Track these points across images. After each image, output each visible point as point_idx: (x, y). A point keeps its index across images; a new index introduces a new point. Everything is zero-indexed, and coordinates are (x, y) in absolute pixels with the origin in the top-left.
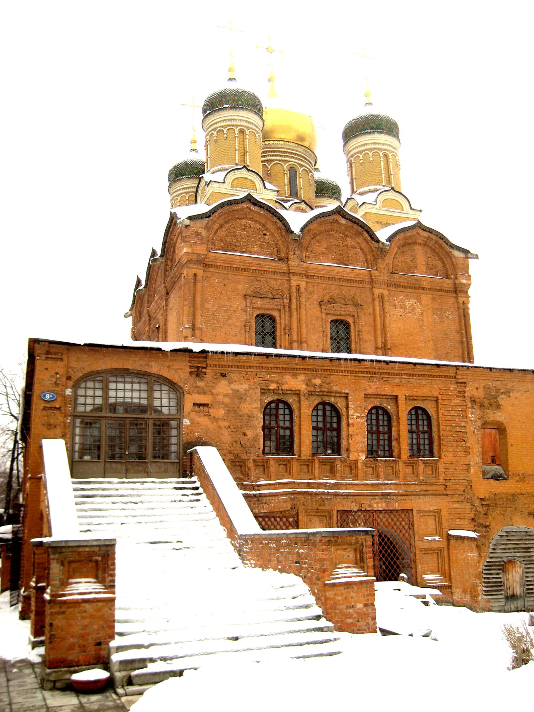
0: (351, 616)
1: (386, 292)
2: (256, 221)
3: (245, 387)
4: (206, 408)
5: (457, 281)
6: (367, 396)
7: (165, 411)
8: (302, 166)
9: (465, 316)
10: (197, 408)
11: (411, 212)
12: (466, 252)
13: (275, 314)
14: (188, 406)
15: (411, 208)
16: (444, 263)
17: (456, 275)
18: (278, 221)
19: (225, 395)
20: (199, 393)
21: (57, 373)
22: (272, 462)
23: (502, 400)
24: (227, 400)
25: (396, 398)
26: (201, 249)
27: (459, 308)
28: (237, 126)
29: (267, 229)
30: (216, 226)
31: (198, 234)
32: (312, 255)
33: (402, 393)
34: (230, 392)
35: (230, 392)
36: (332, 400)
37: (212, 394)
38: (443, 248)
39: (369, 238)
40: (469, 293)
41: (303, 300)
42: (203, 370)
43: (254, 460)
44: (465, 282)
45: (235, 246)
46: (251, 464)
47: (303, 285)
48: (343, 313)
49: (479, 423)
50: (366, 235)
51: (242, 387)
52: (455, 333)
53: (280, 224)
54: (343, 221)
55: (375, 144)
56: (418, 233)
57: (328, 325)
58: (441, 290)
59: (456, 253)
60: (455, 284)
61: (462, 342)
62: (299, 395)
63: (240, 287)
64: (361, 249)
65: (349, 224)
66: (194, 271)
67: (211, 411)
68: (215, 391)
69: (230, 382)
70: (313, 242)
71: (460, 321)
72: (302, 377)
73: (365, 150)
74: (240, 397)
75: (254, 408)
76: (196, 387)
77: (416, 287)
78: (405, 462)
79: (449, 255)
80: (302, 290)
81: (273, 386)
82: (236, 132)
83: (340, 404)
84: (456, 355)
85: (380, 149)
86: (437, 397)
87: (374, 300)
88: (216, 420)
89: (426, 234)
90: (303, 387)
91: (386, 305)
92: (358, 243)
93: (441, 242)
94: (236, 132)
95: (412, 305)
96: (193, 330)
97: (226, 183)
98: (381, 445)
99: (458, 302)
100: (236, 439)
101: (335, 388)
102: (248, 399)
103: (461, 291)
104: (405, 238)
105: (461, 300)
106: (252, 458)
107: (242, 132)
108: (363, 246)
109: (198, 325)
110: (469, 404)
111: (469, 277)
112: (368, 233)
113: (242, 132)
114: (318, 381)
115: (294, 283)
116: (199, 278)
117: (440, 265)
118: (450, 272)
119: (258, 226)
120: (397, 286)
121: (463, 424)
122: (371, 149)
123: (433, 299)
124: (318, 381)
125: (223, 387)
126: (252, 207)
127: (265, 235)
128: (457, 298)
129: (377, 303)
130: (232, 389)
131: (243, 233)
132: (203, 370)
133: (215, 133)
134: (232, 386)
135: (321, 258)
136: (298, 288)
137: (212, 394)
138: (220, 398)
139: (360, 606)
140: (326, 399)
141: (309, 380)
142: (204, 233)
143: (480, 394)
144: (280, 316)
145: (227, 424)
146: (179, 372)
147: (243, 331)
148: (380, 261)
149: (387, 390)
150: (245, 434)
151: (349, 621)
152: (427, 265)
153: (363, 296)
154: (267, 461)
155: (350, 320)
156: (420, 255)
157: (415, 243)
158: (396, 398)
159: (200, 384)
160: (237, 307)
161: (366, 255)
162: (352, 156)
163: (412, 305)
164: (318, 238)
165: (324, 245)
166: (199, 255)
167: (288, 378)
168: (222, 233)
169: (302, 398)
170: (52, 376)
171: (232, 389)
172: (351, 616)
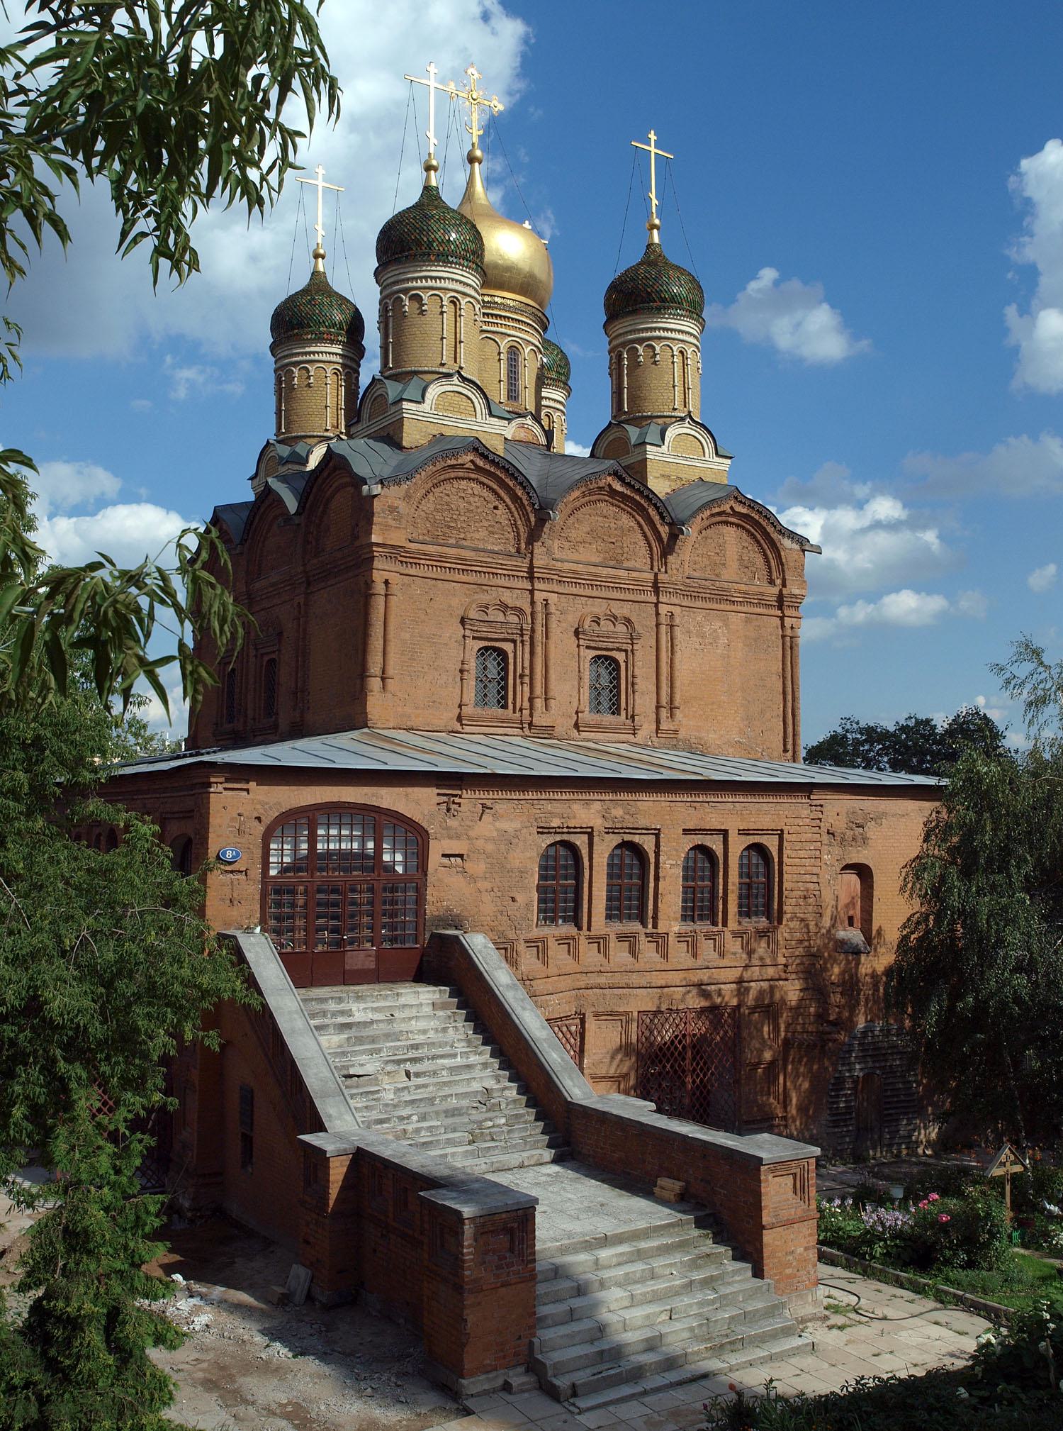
0: (789, 1265)
1: (676, 610)
2: (482, 483)
3: (517, 825)
4: (459, 860)
5: (785, 592)
6: (686, 831)
7: (399, 869)
10: (446, 861)
13: (508, 647)
14: (434, 859)
15: (717, 454)
19: (487, 840)
20: (450, 838)
21: (240, 815)
22: (552, 943)
23: (871, 830)
24: (490, 847)
25: (725, 833)
27: (783, 637)
30: (419, 495)
31: (393, 509)
32: (567, 545)
33: (733, 825)
34: (495, 834)
35: (495, 834)
36: (636, 839)
37: (469, 838)
41: (553, 624)
42: (457, 800)
43: (526, 941)
45: (449, 527)
46: (521, 947)
47: (553, 598)
48: (610, 646)
49: (839, 866)
51: (510, 826)
52: (775, 678)
57: (587, 665)
59: (787, 543)
62: (591, 835)
63: (455, 602)
66: (386, 575)
67: (467, 865)
68: (471, 833)
69: (496, 817)
70: (572, 519)
72: (597, 806)
74: (509, 841)
75: (528, 856)
76: (448, 828)
77: (723, 596)
78: (733, 932)
80: (552, 609)
81: (555, 823)
83: (648, 843)
84: (775, 714)
86: (782, 830)
87: (658, 625)
88: (473, 879)
90: (598, 823)
91: (677, 631)
95: (715, 631)
96: (383, 679)
97: (428, 401)
98: (702, 906)
100: (501, 908)
101: (643, 822)
102: (521, 844)
106: (522, 937)
107: (454, 302)
109: (391, 671)
110: (825, 838)
112: (657, 508)
114: (618, 812)
115: (539, 596)
116: (394, 588)
118: (774, 576)
119: (485, 493)
121: (815, 870)
123: (747, 621)
124: (618, 812)
125: (487, 827)
126: (480, 463)
127: (496, 508)
128: (782, 619)
129: (663, 629)
130: (497, 830)
131: (462, 504)
132: (457, 800)
134: (497, 824)
135: (581, 550)
136: (546, 604)
137: (469, 838)
138: (480, 843)
139: (800, 1250)
140: (627, 838)
141: (607, 810)
142: (403, 507)
143: (840, 825)
144: (515, 653)
145: (487, 885)
146: (417, 803)
147: (458, 679)
149: (714, 822)
150: (513, 900)
151: (789, 1271)
152: (741, 559)
153: (643, 619)
154: (543, 941)
155: (620, 657)
158: (725, 833)
159: (452, 823)
160: (450, 638)
162: (623, 345)
163: (715, 631)
164: (579, 515)
165: (586, 527)
166: (392, 547)
167: (576, 807)
168: (428, 505)
169: (596, 839)
170: (232, 819)
171: (497, 830)
172: (789, 1265)
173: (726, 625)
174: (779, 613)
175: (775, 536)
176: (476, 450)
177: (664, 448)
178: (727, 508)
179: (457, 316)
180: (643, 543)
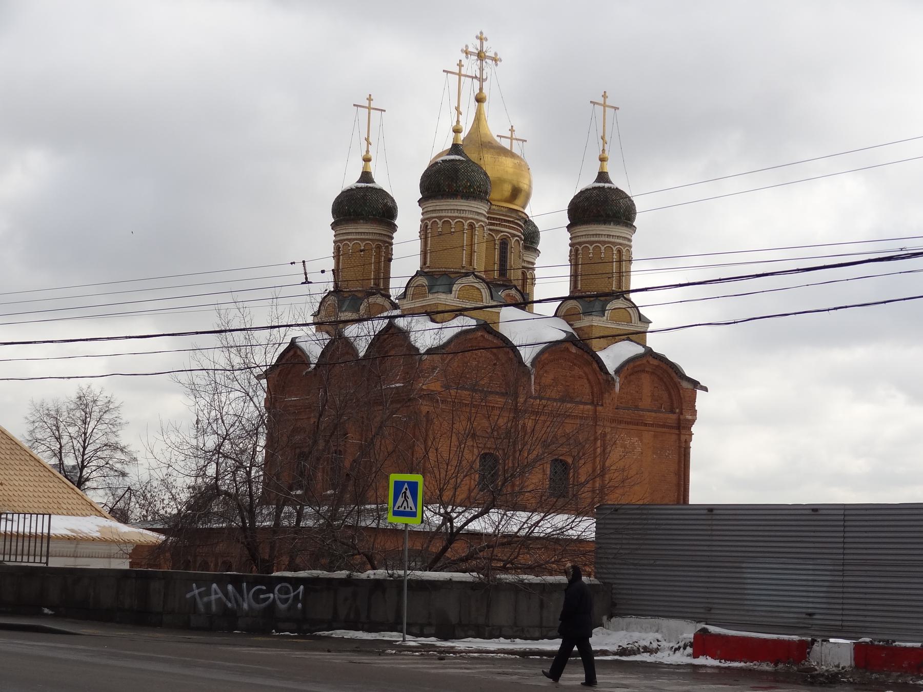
5: (681, 417)
8: (514, 236)
9: (685, 455)
11: (640, 324)
12: (696, 384)
16: (670, 395)
17: (681, 410)
18: (510, 352)
26: (436, 387)
28: (466, 219)
29: (498, 359)
38: (672, 379)
39: (598, 369)
40: (693, 429)
44: (690, 417)
50: (595, 365)
53: (511, 355)
54: (573, 350)
55: (609, 236)
56: (648, 362)
58: (664, 426)
59: (685, 384)
60: (679, 419)
61: (678, 485)
64: (588, 379)
65: (580, 352)
71: (679, 462)
73: (597, 242)
79: (677, 387)
82: (466, 227)
85: (614, 244)
87: (596, 439)
89: (656, 362)
92: (585, 373)
93: (670, 370)
94: (466, 227)
99: (680, 440)
103: (684, 428)
104: (634, 367)
105: (683, 438)
107: (472, 226)
108: (590, 377)
111: (694, 412)
112: (598, 363)
113: (472, 226)
117: (665, 396)
118: (675, 406)
120: (620, 422)
122: (604, 243)
123: (655, 436)
126: (486, 336)
128: (679, 435)
133: (440, 223)
148: (606, 395)
152: (653, 395)
156: (647, 384)
157: (644, 371)
161: (592, 387)
173: (641, 441)
174: (677, 432)
175: (677, 379)
176: (485, 329)
177: (605, 318)
178: (644, 361)
179: (472, 236)
180: (587, 385)
